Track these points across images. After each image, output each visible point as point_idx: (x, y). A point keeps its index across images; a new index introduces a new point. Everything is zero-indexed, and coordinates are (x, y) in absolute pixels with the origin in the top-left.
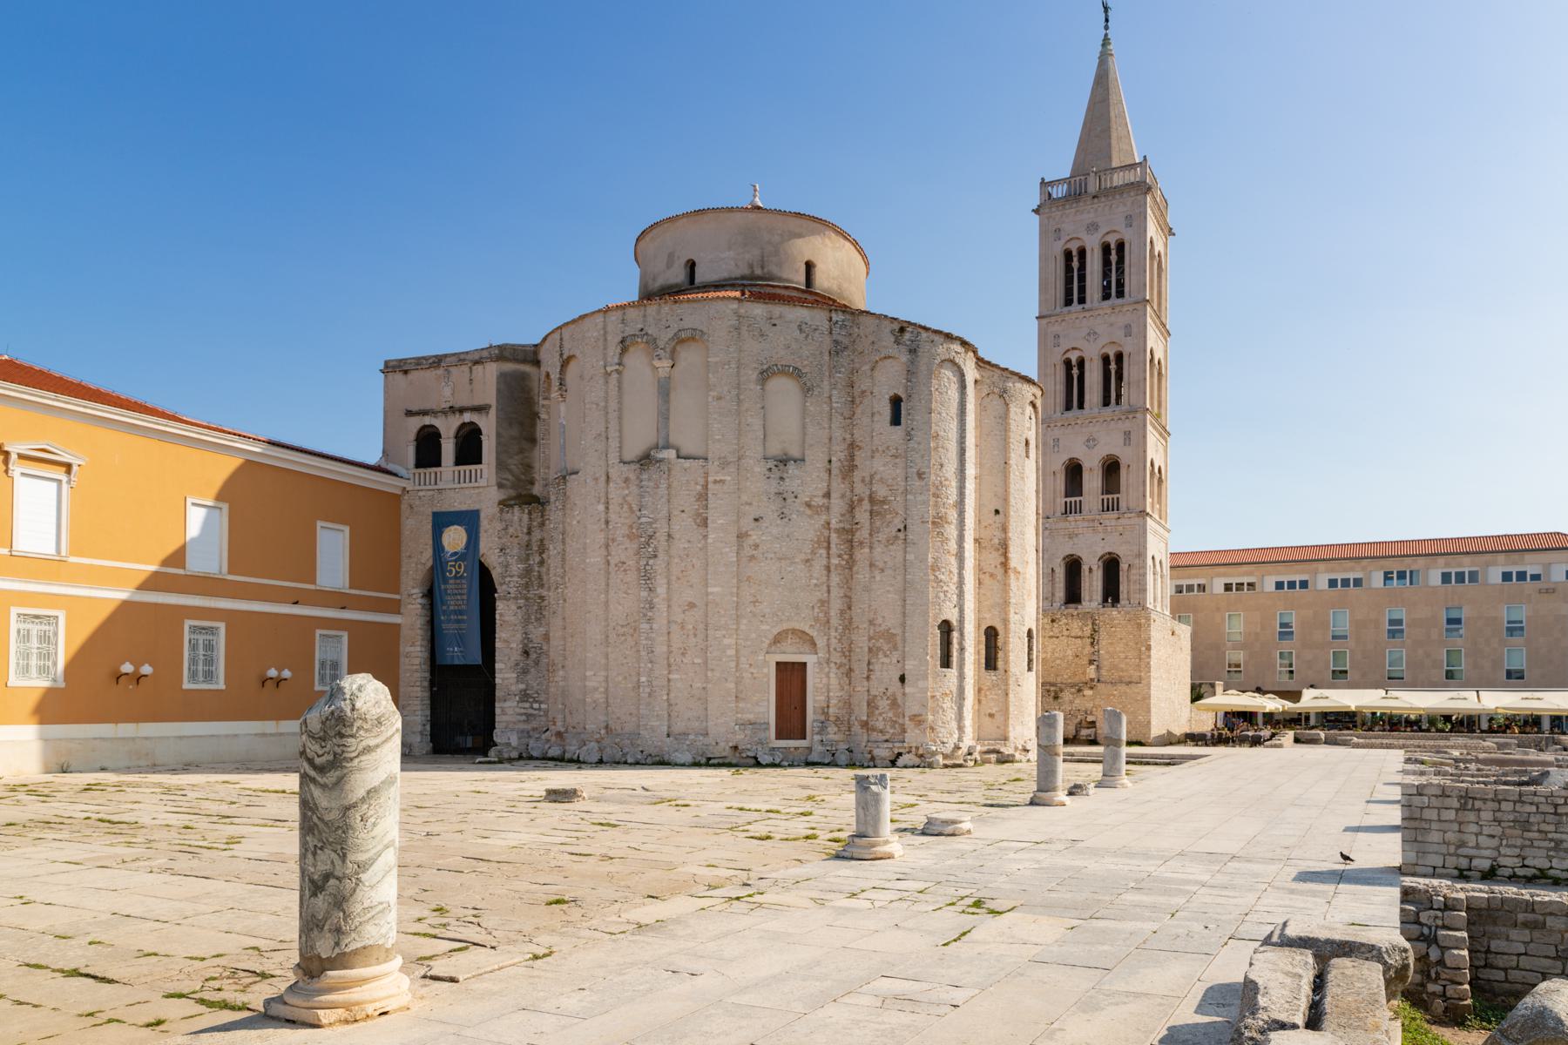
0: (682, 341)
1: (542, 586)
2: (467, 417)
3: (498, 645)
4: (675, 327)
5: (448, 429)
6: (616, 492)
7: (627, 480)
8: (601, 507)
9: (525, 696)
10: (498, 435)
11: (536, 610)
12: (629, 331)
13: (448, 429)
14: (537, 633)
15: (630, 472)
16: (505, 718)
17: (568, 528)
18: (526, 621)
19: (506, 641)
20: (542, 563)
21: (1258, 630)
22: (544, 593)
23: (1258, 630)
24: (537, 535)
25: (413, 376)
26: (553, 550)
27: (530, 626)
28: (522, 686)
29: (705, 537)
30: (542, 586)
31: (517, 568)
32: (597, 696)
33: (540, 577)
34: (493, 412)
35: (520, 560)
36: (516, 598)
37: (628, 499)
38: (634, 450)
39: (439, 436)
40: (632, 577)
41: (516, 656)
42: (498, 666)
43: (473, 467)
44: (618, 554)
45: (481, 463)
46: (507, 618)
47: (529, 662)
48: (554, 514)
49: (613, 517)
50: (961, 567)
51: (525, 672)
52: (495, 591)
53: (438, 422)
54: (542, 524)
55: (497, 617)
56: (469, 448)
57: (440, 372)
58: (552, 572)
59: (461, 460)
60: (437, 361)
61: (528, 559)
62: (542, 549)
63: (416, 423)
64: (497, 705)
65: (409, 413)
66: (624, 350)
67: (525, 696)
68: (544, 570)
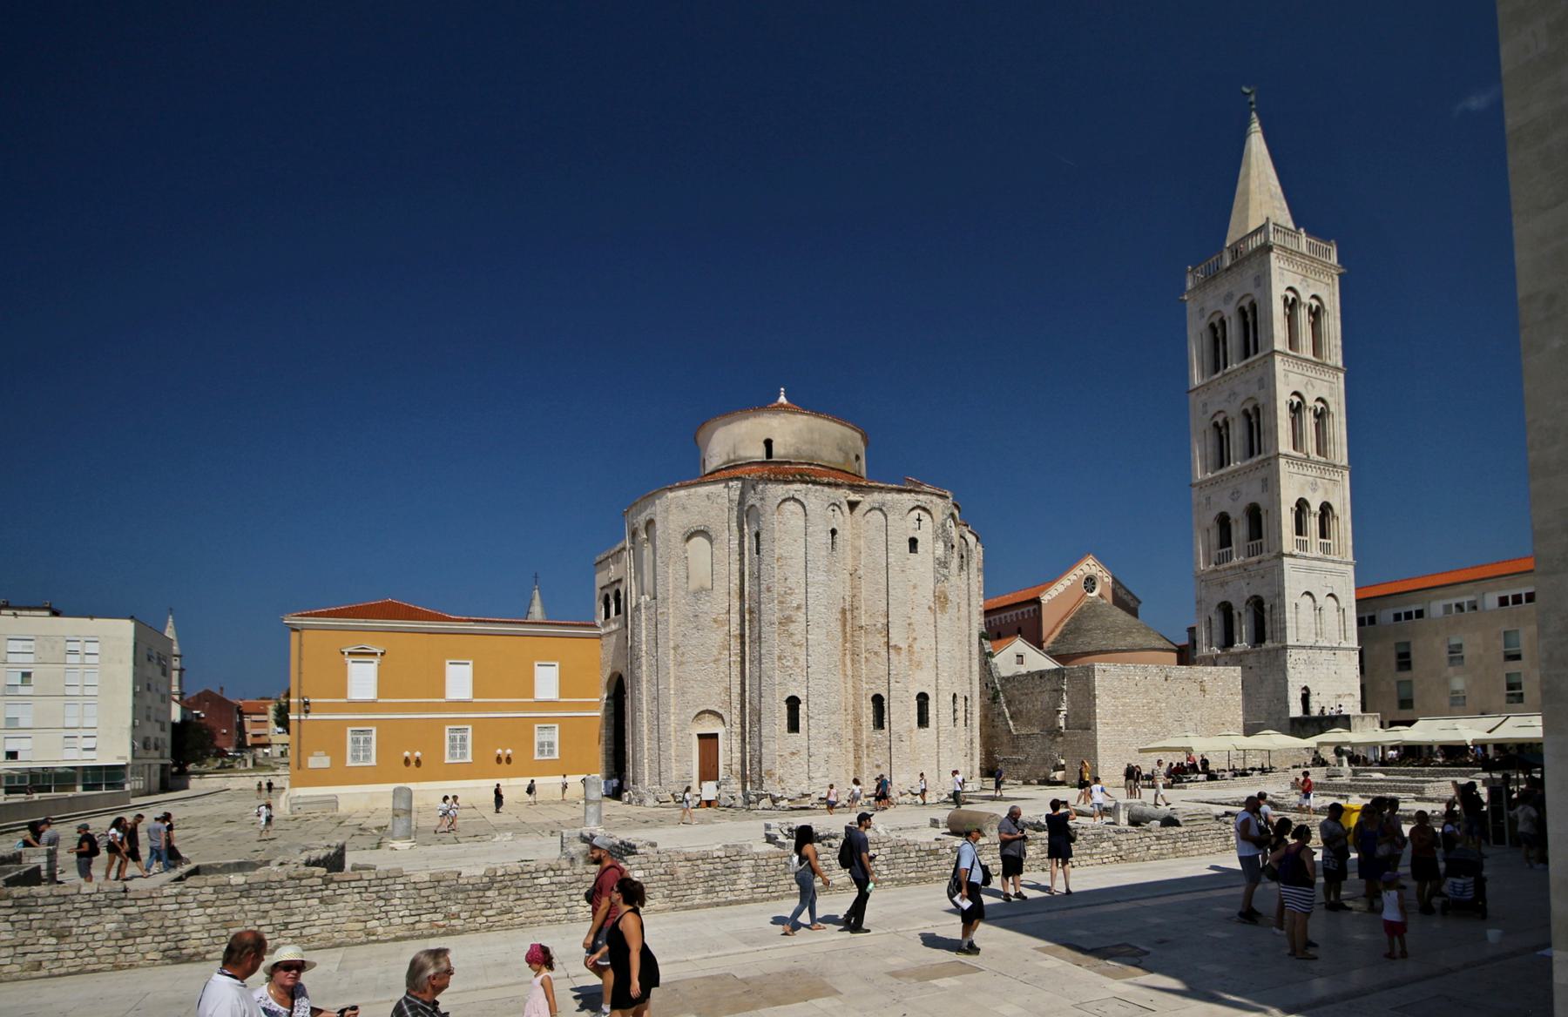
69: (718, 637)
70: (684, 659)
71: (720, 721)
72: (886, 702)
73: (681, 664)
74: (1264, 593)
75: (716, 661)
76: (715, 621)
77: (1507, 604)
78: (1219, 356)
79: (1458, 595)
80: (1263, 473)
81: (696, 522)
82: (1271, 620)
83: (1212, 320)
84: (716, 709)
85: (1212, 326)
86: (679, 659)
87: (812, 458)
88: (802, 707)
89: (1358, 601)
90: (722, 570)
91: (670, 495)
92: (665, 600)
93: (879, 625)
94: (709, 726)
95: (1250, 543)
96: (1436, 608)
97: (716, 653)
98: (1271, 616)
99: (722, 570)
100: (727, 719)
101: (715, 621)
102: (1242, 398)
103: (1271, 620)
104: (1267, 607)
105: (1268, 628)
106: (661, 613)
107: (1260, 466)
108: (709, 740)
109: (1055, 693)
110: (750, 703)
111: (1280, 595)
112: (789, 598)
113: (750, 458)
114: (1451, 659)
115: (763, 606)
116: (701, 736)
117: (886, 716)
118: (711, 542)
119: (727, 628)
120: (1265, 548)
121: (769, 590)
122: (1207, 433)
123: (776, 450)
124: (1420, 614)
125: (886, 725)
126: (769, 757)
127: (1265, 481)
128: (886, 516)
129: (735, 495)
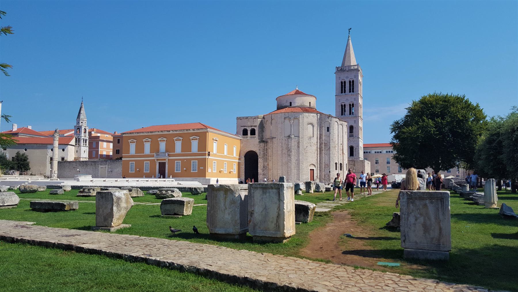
0: (295, 118)
1: (267, 156)
2: (253, 127)
3: (259, 166)
4: (294, 116)
5: (249, 130)
6: (283, 142)
7: (285, 140)
8: (281, 144)
9: (264, 174)
10: (258, 131)
11: (266, 160)
12: (286, 116)
13: (249, 130)
14: (266, 164)
15: (286, 139)
16: (260, 178)
17: (273, 147)
18: (264, 162)
19: (260, 165)
20: (267, 152)
21: (382, 162)
22: (267, 157)
23: (382, 162)
24: (266, 147)
25: (242, 120)
26: (269, 151)
27: (265, 163)
28: (263, 173)
29: (299, 149)
30: (267, 156)
31: (262, 153)
32: (280, 174)
33: (266, 154)
34: (257, 127)
35: (263, 152)
36: (262, 158)
37: (286, 143)
38: (288, 135)
39: (247, 130)
40: (287, 155)
41: (262, 168)
42: (259, 169)
43: (254, 136)
44: (284, 152)
45: (255, 135)
46: (260, 161)
47: (265, 169)
48: (270, 144)
49: (283, 146)
50: (338, 154)
51: (264, 170)
52: (258, 157)
53: (247, 128)
54: (267, 146)
55: (259, 161)
56: (253, 132)
57: (248, 119)
58: (269, 154)
59: (251, 134)
60: (247, 118)
61: (264, 151)
62: (267, 150)
63: (243, 128)
64: (259, 176)
65: (241, 126)
66: (285, 119)
67: (264, 174)
68: (267, 153)
69: (315, 148)
70: (307, 152)
71: (314, 166)
72: (342, 165)
73: (306, 153)
74: (354, 145)
75: (314, 153)
76: (314, 144)
77: (376, 153)
78: (343, 90)
79: (378, 149)
80: (355, 119)
81: (310, 121)
82: (356, 152)
83: (342, 81)
84: (315, 164)
85: (342, 82)
86: (306, 152)
87: (314, 107)
88: (337, 165)
89: (363, 147)
90: (315, 133)
91: (304, 114)
92: (302, 138)
93: (341, 149)
94: (313, 167)
95: (350, 134)
96: (373, 152)
97: (314, 151)
98: (355, 151)
99: (315, 133)
100: (316, 166)
101: (314, 144)
102: (349, 101)
103: (356, 152)
104: (354, 148)
105: (354, 153)
106: (301, 141)
107: (354, 117)
108: (312, 170)
109: (351, 165)
110: (324, 163)
111: (358, 146)
112: (335, 142)
113: (307, 106)
114: (376, 162)
115: (331, 143)
116: (311, 170)
117: (342, 168)
118: (313, 126)
119: (316, 146)
120: (354, 136)
121: (332, 140)
122: (340, 106)
123: (312, 105)
124: (369, 152)
125: (342, 169)
126: (332, 175)
127: (355, 121)
128: (343, 126)
129: (319, 117)
